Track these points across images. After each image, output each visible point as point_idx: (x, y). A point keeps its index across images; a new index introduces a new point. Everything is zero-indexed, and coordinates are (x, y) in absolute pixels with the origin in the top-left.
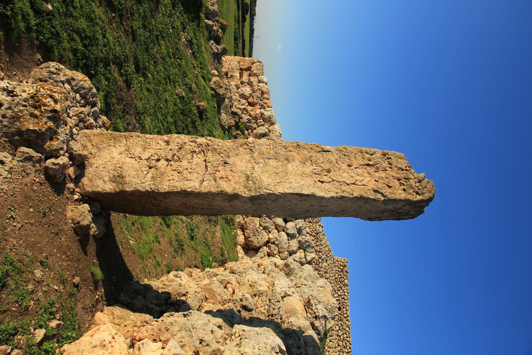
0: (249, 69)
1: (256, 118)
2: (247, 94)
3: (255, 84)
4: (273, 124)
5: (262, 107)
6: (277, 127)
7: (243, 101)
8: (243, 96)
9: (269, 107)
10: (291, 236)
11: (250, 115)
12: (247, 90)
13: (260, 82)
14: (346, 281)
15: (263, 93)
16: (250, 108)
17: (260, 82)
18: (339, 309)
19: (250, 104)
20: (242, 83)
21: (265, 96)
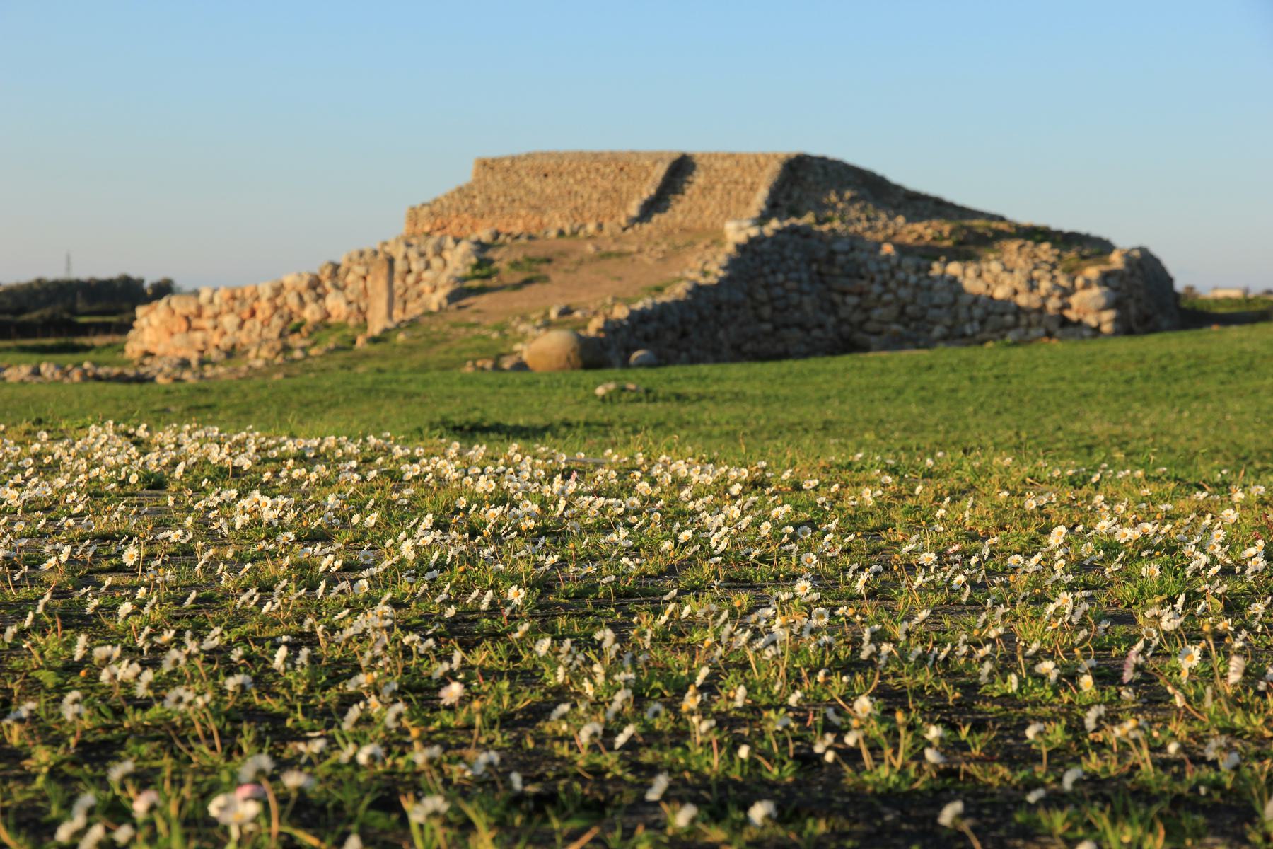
0: (187, 318)
1: (276, 308)
2: (237, 321)
3: (217, 309)
4: (282, 286)
5: (257, 299)
6: (289, 280)
7: (248, 324)
8: (241, 325)
9: (256, 289)
10: (428, 266)
11: (272, 315)
12: (229, 321)
13: (211, 301)
14: (507, 163)
15: (233, 298)
16: (259, 316)
17: (211, 301)
18: (546, 175)
19: (253, 313)
20: (215, 328)
21: (238, 294)
